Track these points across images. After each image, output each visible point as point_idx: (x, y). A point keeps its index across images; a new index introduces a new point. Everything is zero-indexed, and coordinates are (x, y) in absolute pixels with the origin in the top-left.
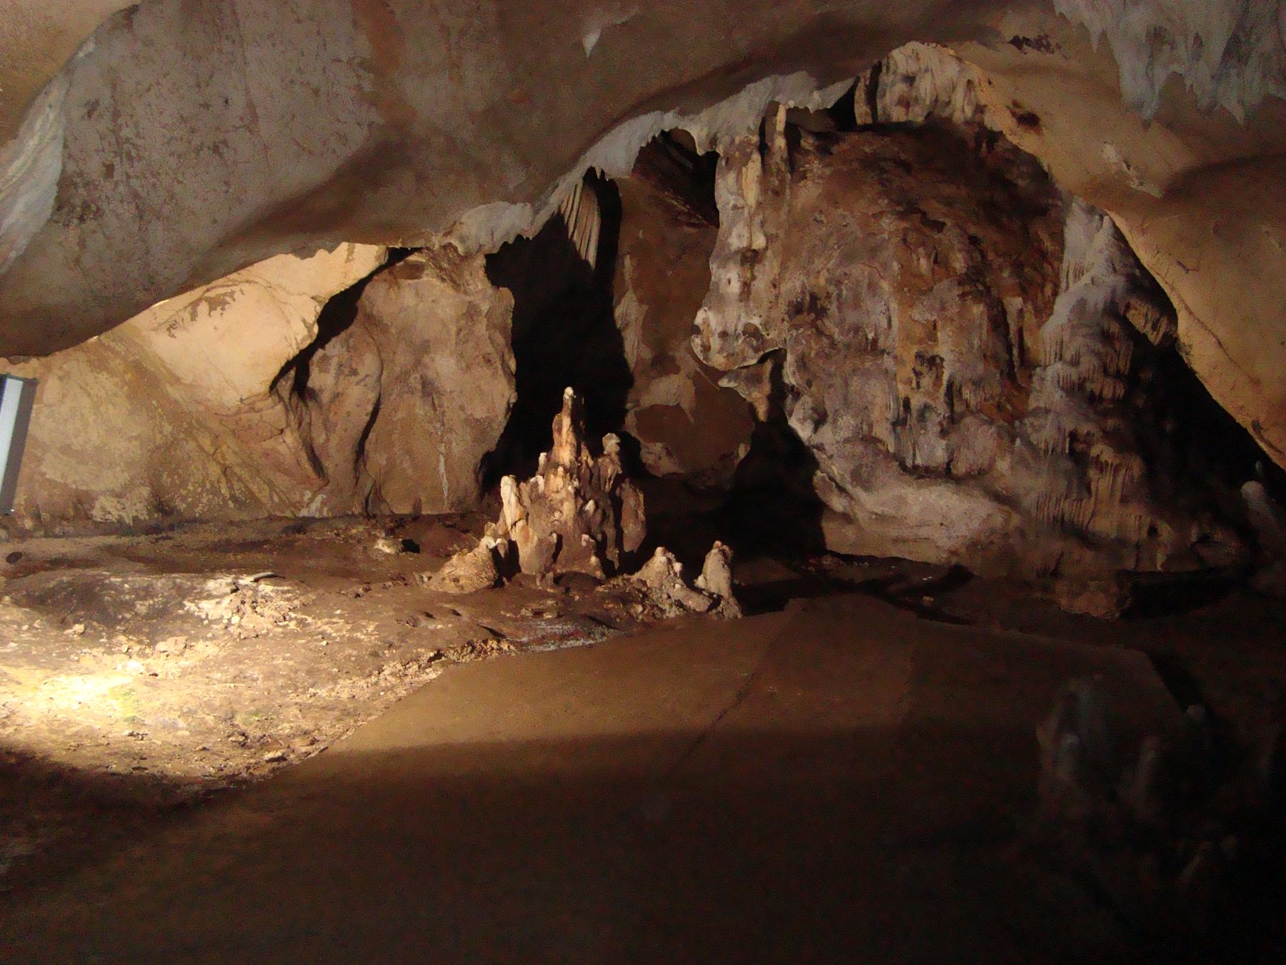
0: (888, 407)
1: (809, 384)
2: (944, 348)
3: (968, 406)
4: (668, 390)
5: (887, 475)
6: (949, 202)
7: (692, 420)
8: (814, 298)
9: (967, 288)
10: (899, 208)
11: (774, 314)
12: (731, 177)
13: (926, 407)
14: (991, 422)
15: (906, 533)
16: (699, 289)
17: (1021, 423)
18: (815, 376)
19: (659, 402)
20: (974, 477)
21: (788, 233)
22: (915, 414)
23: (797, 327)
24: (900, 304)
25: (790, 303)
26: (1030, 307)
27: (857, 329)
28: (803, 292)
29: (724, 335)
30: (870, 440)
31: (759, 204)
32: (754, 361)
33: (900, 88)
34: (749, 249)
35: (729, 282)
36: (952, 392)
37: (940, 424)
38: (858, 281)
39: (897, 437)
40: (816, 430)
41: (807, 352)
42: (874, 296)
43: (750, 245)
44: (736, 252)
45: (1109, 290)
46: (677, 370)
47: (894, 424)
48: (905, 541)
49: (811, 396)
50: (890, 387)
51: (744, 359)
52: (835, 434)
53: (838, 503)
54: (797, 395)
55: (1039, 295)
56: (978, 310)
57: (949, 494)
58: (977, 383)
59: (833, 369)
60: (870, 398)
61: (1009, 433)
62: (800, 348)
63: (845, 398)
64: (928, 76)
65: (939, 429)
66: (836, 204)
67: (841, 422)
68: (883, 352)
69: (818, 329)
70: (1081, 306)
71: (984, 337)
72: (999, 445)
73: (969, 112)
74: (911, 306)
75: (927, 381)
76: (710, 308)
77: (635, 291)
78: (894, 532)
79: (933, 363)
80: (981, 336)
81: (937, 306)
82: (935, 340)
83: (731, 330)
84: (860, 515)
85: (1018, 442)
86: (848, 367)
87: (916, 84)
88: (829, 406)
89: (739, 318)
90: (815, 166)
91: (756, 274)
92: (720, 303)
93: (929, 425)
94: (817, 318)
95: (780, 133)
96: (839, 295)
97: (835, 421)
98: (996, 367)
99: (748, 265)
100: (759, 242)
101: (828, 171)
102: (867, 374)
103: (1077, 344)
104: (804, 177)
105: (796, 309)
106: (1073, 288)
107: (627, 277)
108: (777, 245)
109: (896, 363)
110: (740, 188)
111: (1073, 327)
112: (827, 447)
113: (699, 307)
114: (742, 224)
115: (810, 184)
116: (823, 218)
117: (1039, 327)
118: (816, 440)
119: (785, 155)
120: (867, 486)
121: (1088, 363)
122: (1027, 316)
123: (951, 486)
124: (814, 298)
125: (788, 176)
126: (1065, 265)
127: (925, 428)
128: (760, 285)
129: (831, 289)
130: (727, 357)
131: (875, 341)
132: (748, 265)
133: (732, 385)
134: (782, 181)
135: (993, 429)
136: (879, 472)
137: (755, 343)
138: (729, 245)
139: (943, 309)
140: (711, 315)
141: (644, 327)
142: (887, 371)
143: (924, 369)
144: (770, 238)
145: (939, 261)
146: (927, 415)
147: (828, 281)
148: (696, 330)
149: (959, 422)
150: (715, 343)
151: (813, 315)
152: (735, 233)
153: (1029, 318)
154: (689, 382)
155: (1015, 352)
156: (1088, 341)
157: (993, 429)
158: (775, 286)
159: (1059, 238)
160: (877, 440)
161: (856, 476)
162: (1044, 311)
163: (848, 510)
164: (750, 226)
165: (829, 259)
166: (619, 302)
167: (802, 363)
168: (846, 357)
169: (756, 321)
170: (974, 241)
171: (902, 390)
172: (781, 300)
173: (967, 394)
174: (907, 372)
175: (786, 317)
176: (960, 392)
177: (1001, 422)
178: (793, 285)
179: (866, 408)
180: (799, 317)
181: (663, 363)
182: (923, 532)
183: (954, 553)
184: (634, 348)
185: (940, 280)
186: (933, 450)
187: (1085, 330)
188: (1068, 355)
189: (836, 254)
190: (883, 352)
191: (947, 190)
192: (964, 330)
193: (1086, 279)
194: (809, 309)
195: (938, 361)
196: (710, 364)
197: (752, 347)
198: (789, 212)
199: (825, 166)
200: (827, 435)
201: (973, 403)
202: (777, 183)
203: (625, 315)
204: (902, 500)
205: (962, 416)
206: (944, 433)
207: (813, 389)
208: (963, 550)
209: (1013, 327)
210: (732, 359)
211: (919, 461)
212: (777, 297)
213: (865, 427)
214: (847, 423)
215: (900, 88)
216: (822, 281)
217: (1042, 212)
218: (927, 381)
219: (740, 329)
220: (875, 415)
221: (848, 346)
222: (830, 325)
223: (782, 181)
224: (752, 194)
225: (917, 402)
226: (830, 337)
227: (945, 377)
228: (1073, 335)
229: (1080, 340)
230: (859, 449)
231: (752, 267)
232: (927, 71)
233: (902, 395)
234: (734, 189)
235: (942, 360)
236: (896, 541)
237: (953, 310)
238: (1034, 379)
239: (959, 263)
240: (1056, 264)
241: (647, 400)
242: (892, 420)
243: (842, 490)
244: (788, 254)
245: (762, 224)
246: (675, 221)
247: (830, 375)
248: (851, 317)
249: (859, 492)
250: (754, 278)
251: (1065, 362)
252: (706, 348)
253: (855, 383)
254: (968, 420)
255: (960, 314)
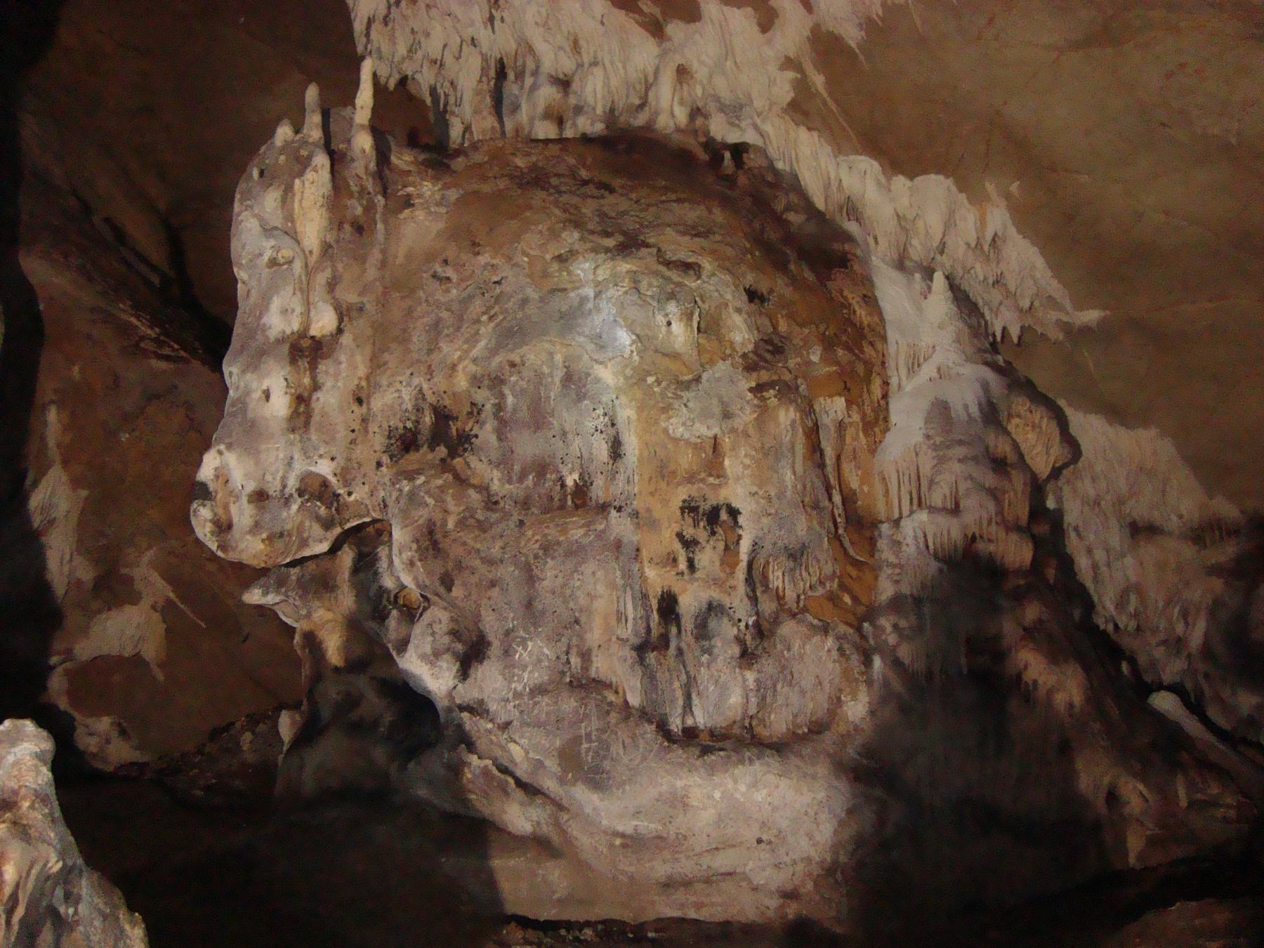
0: (621, 617)
1: (447, 582)
2: (738, 490)
3: (780, 598)
4: (127, 630)
5: (632, 748)
6: (695, 231)
7: (160, 677)
8: (442, 416)
9: (765, 376)
10: (610, 242)
11: (360, 452)
12: (270, 200)
13: (713, 609)
14: (825, 630)
15: (686, 867)
16: (205, 417)
17: (873, 624)
18: (459, 566)
19: (105, 651)
20: (803, 738)
21: (383, 303)
22: (688, 623)
23: (410, 476)
24: (641, 409)
25: (390, 434)
26: (856, 417)
27: (541, 468)
28: (418, 410)
29: (260, 497)
30: (587, 685)
31: (326, 248)
32: (324, 547)
33: (547, 94)
34: (303, 334)
35: (267, 395)
36: (755, 580)
37: (739, 640)
38: (539, 376)
39: (650, 677)
40: (464, 674)
41: (438, 516)
42: (581, 397)
43: (306, 327)
44: (280, 341)
45: (978, 386)
46: (134, 599)
47: (641, 649)
48: (687, 883)
49: (452, 605)
50: (627, 575)
51: (304, 543)
52: (509, 679)
53: (519, 817)
54: (411, 614)
55: (865, 396)
56: (786, 416)
57: (771, 778)
58: (796, 555)
59: (496, 551)
60: (583, 601)
61: (858, 648)
62: (421, 515)
63: (529, 605)
64: (598, 71)
65: (736, 650)
66: (475, 247)
67: (520, 654)
68: (603, 508)
69: (457, 476)
70: (941, 412)
71: (799, 468)
72: (846, 673)
73: (681, 115)
74: (666, 409)
75: (708, 557)
76: (229, 447)
77: (65, 463)
78: (661, 869)
79: (718, 518)
80: (791, 474)
81: (717, 410)
82: (721, 475)
83: (273, 487)
84: (584, 841)
85: (877, 662)
86: (531, 542)
87: (575, 86)
88: (491, 626)
89: (290, 462)
90: (428, 189)
91: (321, 378)
92: (252, 435)
93: (717, 642)
94: (453, 453)
95: (362, 126)
96: (499, 407)
97: (507, 652)
98: (821, 524)
99: (304, 363)
100: (324, 322)
101: (453, 195)
102: (576, 552)
103: (954, 475)
104: (407, 203)
105: (406, 442)
106: (908, 387)
107: (51, 443)
108: (362, 324)
109: (638, 526)
110: (290, 218)
111: (935, 447)
112: (493, 707)
113: (207, 447)
114: (290, 289)
115: (420, 215)
116: (450, 272)
117: (873, 451)
118: (467, 693)
119: (372, 166)
120: (597, 779)
121: (977, 510)
122: (850, 432)
123: (773, 761)
124: (442, 416)
125: (380, 200)
126: (892, 349)
127: (709, 651)
128: (330, 399)
129: (481, 396)
130: (270, 539)
131: (581, 491)
132: (304, 363)
133: (271, 599)
134: (369, 208)
135: (830, 642)
136: (616, 749)
137: (323, 511)
138: (264, 329)
139: (727, 415)
140: (231, 459)
141: (82, 525)
142: (618, 545)
143: (701, 534)
144: (343, 313)
145: (709, 327)
146: (712, 624)
147: (476, 381)
148: (203, 492)
149: (773, 633)
150: (243, 514)
151: (442, 451)
152: (276, 304)
153: (856, 439)
154: (156, 616)
155: (837, 498)
156: (971, 468)
157: (830, 642)
158: (360, 401)
159: (870, 301)
160: (600, 685)
161: (570, 759)
162: (877, 422)
163: (546, 829)
164: (305, 291)
165: (474, 339)
166: (36, 483)
167: (431, 542)
168: (521, 523)
169: (325, 468)
170: (753, 295)
171: (656, 579)
172: (373, 427)
173: (777, 578)
174: (666, 540)
175: (385, 459)
176: (765, 577)
177: (843, 628)
178: (396, 398)
179: (577, 622)
180: (413, 456)
181: (111, 588)
182: (723, 862)
183: (790, 895)
184: (63, 561)
185: (712, 362)
186: (723, 693)
187: (960, 451)
188: (937, 497)
189: (487, 330)
190: (603, 508)
191: (692, 213)
192: (770, 454)
193: (928, 370)
194: (436, 437)
195: (724, 516)
196: (232, 556)
197: (318, 518)
198: (383, 264)
199: (446, 187)
200: (489, 681)
201: (790, 595)
202: (359, 210)
203: (46, 508)
204: (679, 802)
205: (776, 621)
206: (747, 657)
207: (457, 592)
208: (810, 886)
209: (829, 453)
210: (279, 544)
211: (700, 718)
212: (364, 420)
213: (575, 661)
214: (536, 655)
215: (547, 94)
216: (462, 382)
217: (843, 261)
218: (708, 557)
219: (293, 483)
220: (594, 636)
221: (525, 504)
222: (480, 467)
223: (369, 208)
224: (313, 227)
225: (690, 601)
226: (484, 489)
227: (745, 547)
228: (941, 460)
229: (957, 467)
230: (569, 704)
231: (313, 367)
232: (595, 63)
233: (655, 591)
234: (277, 220)
235: (734, 513)
236: (669, 885)
237: (746, 417)
238: (882, 544)
239: (740, 332)
240: (879, 346)
241: (85, 650)
242: (636, 641)
243: (530, 790)
244: (386, 340)
245: (332, 286)
246: (135, 349)
247: (490, 562)
248: (527, 446)
249: (583, 796)
250: (316, 387)
251: (932, 510)
252: (223, 527)
253: (551, 574)
254: (788, 628)
255: (760, 422)
